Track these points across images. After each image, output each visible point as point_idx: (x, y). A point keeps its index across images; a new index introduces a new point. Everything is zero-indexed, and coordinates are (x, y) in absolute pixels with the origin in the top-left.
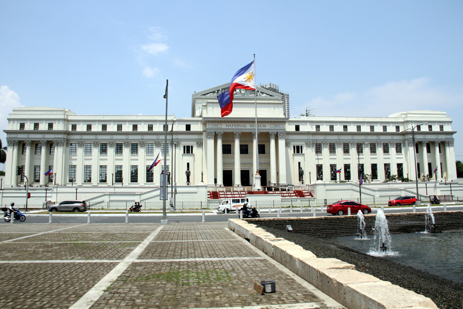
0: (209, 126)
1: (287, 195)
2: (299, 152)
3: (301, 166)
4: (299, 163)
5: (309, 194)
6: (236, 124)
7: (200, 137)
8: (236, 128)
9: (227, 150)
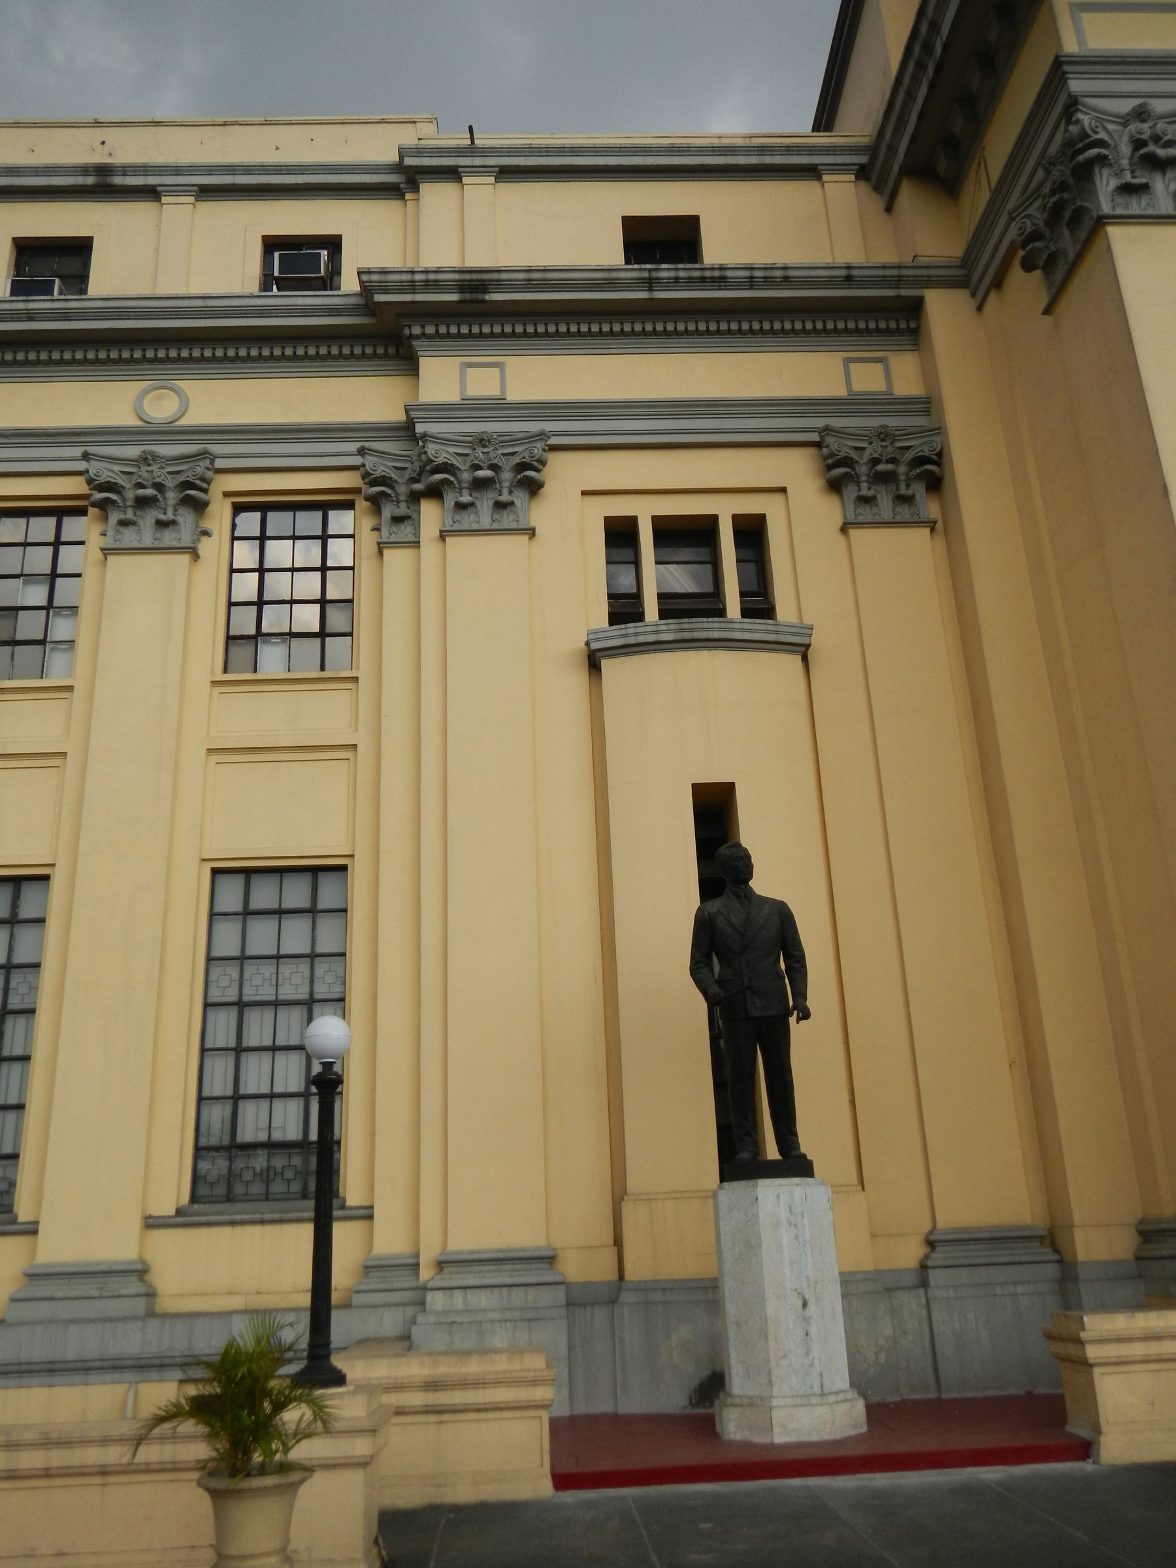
7: (868, 378)
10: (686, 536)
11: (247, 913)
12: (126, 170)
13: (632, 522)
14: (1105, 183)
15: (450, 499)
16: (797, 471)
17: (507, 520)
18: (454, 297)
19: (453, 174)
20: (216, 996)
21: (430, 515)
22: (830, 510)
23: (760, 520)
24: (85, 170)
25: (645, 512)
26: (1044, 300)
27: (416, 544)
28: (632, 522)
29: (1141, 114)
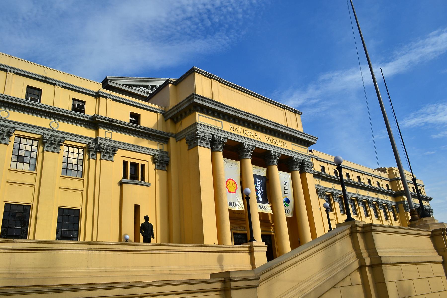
8: (245, 136)
10: (134, 165)
12: (50, 79)
13: (127, 162)
14: (199, 141)
15: (102, 154)
18: (108, 122)
19: (106, 97)
21: (99, 156)
23: (144, 165)
24: (43, 77)
25: (129, 161)
26: (188, 149)
28: (127, 162)
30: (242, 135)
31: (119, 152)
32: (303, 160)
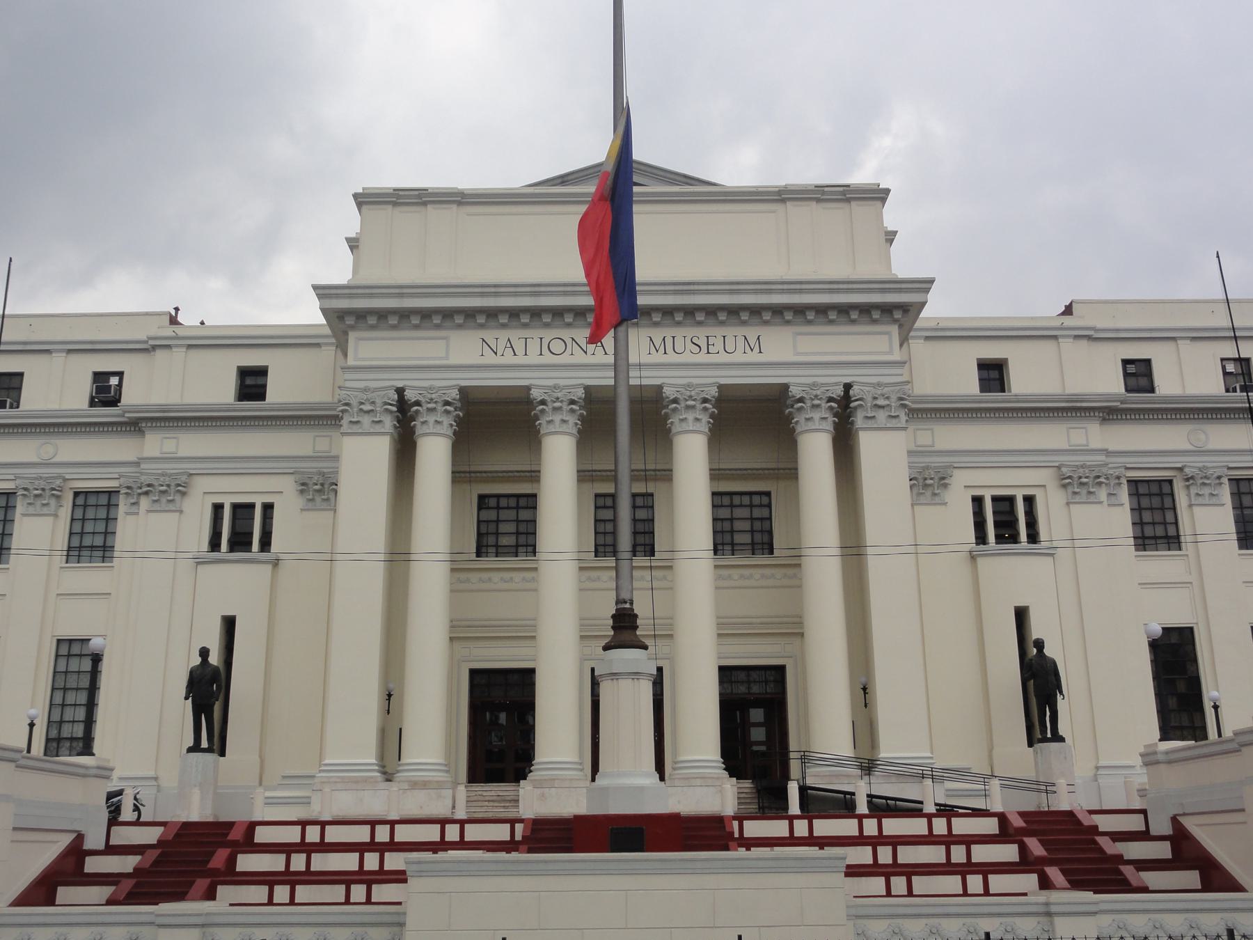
0: (369, 348)
1: (934, 854)
2: (1014, 539)
3: (1035, 632)
4: (1021, 615)
5: (1163, 850)
6: (548, 334)
8: (548, 359)
9: (502, 526)
10: (243, 511)
11: (69, 656)
16: (287, 485)
17: (171, 507)
19: (168, 347)
20: (57, 686)
21: (145, 503)
22: (299, 502)
25: (227, 502)
27: (137, 513)
29: (365, 390)
30: (533, 358)
31: (202, 485)
32: (848, 387)
